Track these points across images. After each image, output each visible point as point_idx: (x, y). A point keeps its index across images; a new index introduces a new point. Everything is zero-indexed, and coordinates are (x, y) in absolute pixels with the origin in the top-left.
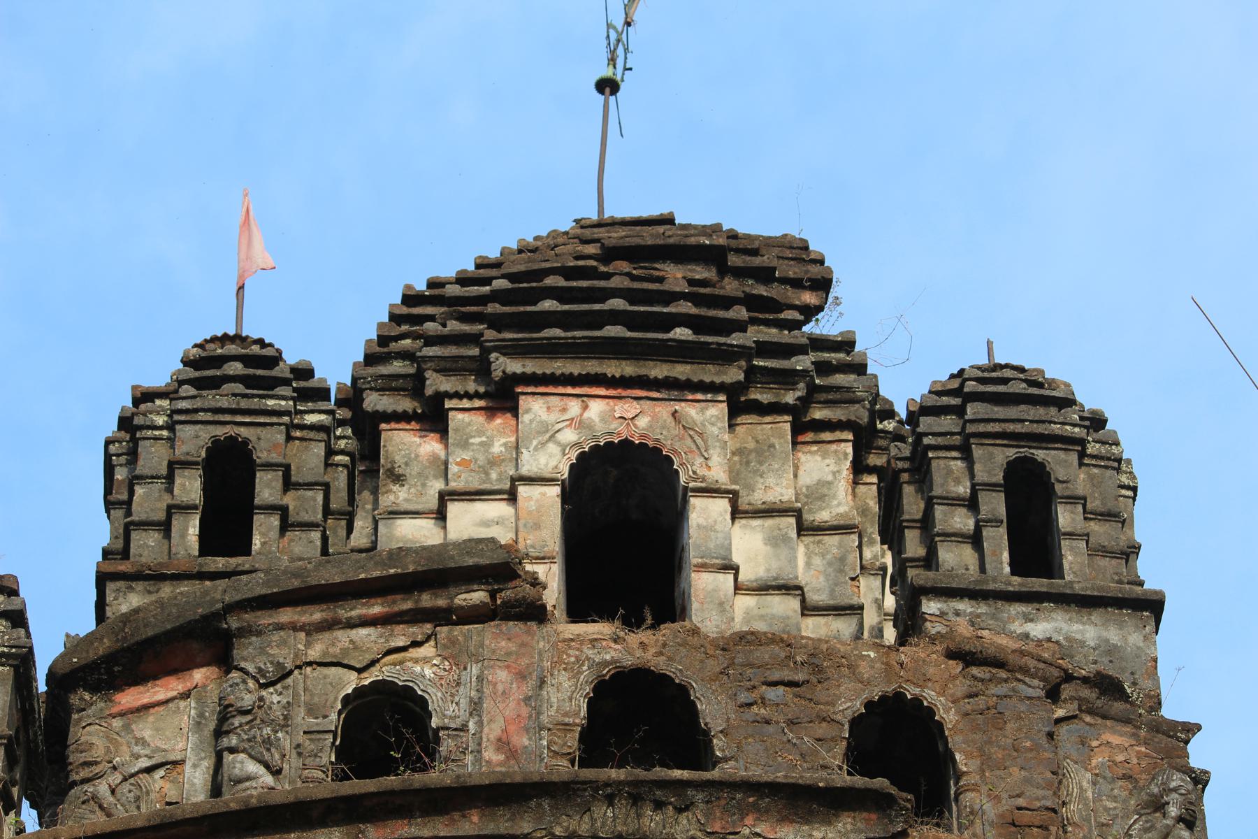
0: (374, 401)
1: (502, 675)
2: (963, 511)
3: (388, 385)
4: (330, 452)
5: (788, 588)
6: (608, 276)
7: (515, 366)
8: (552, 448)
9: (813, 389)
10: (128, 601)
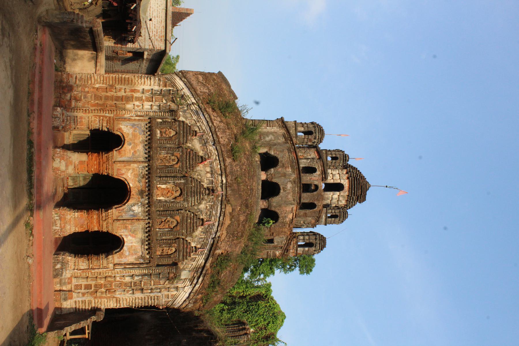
0: (348, 169)
1: (317, 178)
3: (350, 170)
5: (332, 199)
7: (350, 179)
9: (350, 202)
10: (324, 152)
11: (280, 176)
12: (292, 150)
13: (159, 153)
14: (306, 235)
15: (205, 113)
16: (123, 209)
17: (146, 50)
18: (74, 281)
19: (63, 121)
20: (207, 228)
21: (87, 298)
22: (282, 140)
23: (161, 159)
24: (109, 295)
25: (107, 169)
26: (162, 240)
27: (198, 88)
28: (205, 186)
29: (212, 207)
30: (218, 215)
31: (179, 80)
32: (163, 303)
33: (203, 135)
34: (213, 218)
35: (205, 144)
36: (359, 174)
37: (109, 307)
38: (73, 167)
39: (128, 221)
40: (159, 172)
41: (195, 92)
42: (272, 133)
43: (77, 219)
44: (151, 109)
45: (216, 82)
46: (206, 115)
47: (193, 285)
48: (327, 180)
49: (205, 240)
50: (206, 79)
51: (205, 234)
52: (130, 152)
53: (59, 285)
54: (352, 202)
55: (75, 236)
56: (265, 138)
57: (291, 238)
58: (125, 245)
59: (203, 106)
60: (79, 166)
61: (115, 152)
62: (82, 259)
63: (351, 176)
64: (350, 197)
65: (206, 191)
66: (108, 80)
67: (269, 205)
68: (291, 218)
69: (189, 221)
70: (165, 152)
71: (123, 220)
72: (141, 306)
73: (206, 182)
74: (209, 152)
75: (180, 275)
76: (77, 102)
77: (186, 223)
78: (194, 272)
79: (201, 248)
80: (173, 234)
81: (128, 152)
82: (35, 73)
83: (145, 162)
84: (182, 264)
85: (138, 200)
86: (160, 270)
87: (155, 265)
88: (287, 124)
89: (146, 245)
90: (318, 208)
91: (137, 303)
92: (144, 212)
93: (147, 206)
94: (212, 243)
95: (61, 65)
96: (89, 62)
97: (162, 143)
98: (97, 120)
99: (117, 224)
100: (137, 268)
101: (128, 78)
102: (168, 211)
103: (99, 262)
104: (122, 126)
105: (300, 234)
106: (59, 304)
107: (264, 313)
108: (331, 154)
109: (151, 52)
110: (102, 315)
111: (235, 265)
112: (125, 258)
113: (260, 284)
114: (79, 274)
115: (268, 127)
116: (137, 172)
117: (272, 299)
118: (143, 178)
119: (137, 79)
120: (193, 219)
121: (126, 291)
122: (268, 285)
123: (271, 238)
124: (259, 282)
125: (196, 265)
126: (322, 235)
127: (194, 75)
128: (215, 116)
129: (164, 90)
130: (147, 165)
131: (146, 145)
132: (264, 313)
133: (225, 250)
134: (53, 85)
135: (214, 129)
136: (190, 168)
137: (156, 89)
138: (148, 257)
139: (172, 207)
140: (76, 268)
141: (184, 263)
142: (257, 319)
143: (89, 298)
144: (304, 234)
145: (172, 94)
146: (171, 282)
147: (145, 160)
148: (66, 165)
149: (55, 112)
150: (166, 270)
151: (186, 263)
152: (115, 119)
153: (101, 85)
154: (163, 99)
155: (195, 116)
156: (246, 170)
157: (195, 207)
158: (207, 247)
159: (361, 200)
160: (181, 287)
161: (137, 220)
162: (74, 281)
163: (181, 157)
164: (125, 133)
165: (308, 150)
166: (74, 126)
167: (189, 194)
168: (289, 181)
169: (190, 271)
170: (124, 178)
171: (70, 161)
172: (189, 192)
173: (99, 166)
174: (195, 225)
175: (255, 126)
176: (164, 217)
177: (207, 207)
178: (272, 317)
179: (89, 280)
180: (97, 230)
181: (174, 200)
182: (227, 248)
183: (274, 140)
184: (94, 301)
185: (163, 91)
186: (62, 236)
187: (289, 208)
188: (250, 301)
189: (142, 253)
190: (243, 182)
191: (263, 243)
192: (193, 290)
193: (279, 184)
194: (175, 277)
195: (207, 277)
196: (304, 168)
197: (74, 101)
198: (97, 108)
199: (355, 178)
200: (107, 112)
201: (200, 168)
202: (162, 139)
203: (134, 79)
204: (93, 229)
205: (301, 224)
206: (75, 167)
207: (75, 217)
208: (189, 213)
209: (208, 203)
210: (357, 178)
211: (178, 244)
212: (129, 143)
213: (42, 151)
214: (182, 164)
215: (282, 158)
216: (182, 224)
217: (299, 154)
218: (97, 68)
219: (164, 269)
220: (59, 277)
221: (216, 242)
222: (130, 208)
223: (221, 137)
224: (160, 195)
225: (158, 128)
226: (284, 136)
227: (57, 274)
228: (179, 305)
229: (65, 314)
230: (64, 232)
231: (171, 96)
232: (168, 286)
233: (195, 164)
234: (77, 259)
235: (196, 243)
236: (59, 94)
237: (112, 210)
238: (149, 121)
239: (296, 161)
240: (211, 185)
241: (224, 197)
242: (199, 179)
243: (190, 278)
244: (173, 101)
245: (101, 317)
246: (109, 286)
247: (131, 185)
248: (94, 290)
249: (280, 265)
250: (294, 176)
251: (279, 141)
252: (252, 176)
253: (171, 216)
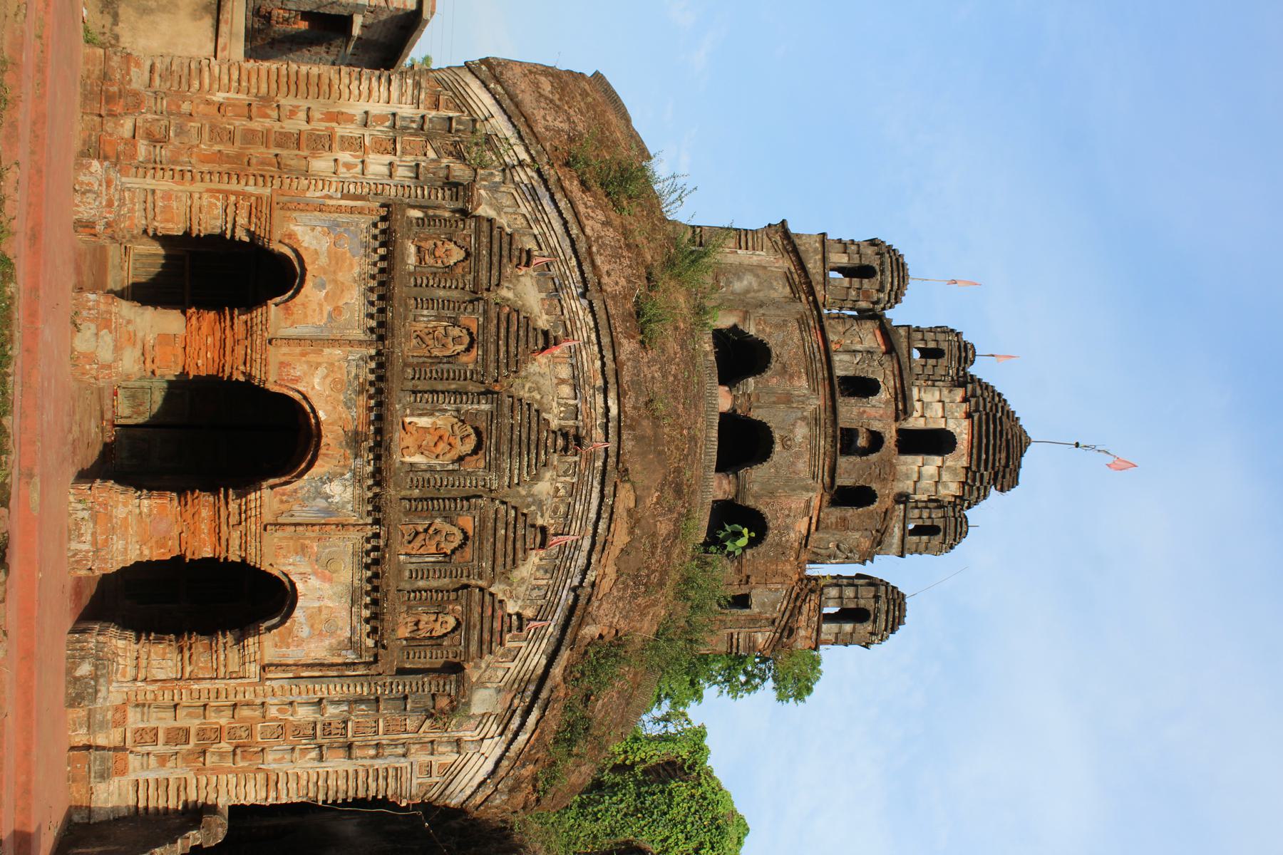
0: (970, 387)
1: (881, 412)
2: (928, 515)
3: (974, 390)
4: (944, 376)
5: (919, 478)
6: (1001, 440)
7: (976, 416)
8: (955, 426)
9: (972, 486)
10: (902, 332)
11: (774, 403)
12: (812, 323)
13: (411, 317)
14: (846, 586)
15: (558, 196)
16: (295, 491)
17: (359, 8)
18: (134, 719)
19: (110, 204)
20: (557, 558)
21: (174, 772)
22: (782, 291)
23: (418, 336)
24: (246, 764)
25: (245, 364)
26: (414, 591)
27: (539, 115)
28: (555, 424)
29: (573, 490)
30: (593, 515)
31: (480, 88)
32: (414, 792)
33: (552, 263)
34: (575, 526)
35: (557, 291)
36: (1000, 405)
37: (243, 802)
38: (138, 353)
39: (309, 528)
40: (411, 377)
41: (530, 126)
42: (752, 269)
43: (148, 520)
44: (391, 176)
45: (590, 100)
46: (560, 200)
47: (510, 736)
48: (911, 419)
49: (549, 593)
50: (563, 89)
51: (548, 575)
52: (321, 310)
53: (84, 730)
54: (978, 489)
55: (141, 568)
56: (731, 282)
57: (803, 595)
58: (298, 605)
59: (552, 172)
60: (156, 349)
61: (274, 309)
62: (161, 646)
63: (977, 410)
64: (975, 473)
65: (556, 441)
66: (254, 81)
67: (740, 489)
68: (804, 532)
69: (503, 532)
70: (433, 313)
71: (296, 525)
72: (345, 800)
73: (556, 411)
74: (567, 316)
75: (468, 704)
76: (155, 146)
77: (492, 540)
78: (512, 695)
79: (535, 620)
80: (451, 572)
81: (314, 310)
82: (22, 36)
83: (369, 344)
84: (477, 667)
85: (342, 463)
86: (407, 687)
87: (392, 670)
88: (797, 241)
89: (366, 606)
90: (880, 503)
91: (330, 787)
92: (362, 500)
93: (370, 482)
94: (570, 602)
95: (104, 26)
96: (195, 20)
97: (421, 286)
98: (219, 204)
99: (274, 538)
100: (336, 679)
101: (319, 76)
102: (438, 499)
103: (215, 657)
104: (296, 228)
105: (831, 581)
106: (83, 791)
107: (686, 816)
108: (923, 340)
109: (373, 15)
110: (221, 825)
111: (636, 674)
112: (298, 646)
113: (671, 729)
114: (150, 697)
115: (740, 248)
116: (342, 374)
117: (709, 774)
118: (360, 392)
119: (347, 81)
120: (515, 527)
121: (297, 751)
122: (695, 733)
123: (743, 590)
124: (669, 724)
125: (519, 672)
126: (894, 588)
127: (525, 75)
128: (589, 204)
129: (430, 119)
130: (373, 352)
131: (371, 290)
132: (686, 816)
133: (611, 627)
134: (79, 90)
135: (585, 245)
136: (507, 364)
137: (405, 115)
138: (370, 643)
139: (449, 487)
140: (141, 676)
141: (483, 666)
142: (667, 834)
143: (178, 770)
144: (840, 582)
145: (457, 131)
146: (440, 724)
147: (367, 338)
148: (116, 346)
149: (85, 175)
150: (428, 684)
151: (488, 666)
152: (274, 205)
153: (232, 95)
154: (429, 147)
155: (527, 204)
156: (679, 377)
157: (520, 489)
158: (556, 617)
159: (1005, 484)
161: (340, 527)
162: (134, 719)
163: (480, 332)
164: (306, 249)
165: (855, 324)
166: (144, 222)
167: (505, 448)
168: (800, 419)
169: (499, 690)
170: (299, 392)
171: (129, 333)
172: (505, 439)
173: (222, 351)
174: (519, 545)
175: (701, 244)
176: (425, 518)
177: (557, 490)
178: (709, 831)
179: (181, 713)
180: (211, 555)
181: (456, 466)
182: (616, 620)
183: (759, 291)
184: (195, 781)
185: (427, 121)
186: (98, 573)
187: (797, 503)
188: (645, 781)
189: (353, 629)
190: (669, 415)
191: (716, 607)
192: (507, 749)
193: (769, 427)
194: (453, 709)
195: (554, 709)
196: (845, 380)
197: (146, 142)
198: (217, 168)
199: (991, 417)
200: (252, 181)
201: (540, 366)
202: (422, 274)
203: (337, 82)
204: (196, 554)
205: (828, 552)
206: (143, 354)
207: (140, 513)
208: (503, 507)
209: (563, 479)
210: (994, 416)
211: (464, 602)
212: (318, 280)
213: (41, 293)
214: (485, 352)
215: (782, 347)
216: (481, 543)
217: (832, 337)
218: (221, 41)
219: (420, 683)
220: (86, 703)
221: (582, 601)
222: (316, 488)
223: (607, 272)
224: (412, 450)
225: (412, 236)
226: (788, 279)
227: (81, 693)
228: (465, 798)
229: (101, 823)
230: (105, 560)
231: (452, 139)
232: (431, 736)
233: (524, 355)
234: (143, 648)
235: (520, 603)
236: (97, 119)
237: (259, 493)
238: (383, 212)
239: (823, 358)
240: (571, 423)
241: (612, 460)
242: (536, 401)
243: (499, 711)
244: (460, 157)
245: (216, 834)
246: (244, 735)
247: (321, 414)
248: (197, 745)
249: (720, 674)
250: (816, 402)
251: (774, 295)
252: (696, 399)
253: (445, 517)
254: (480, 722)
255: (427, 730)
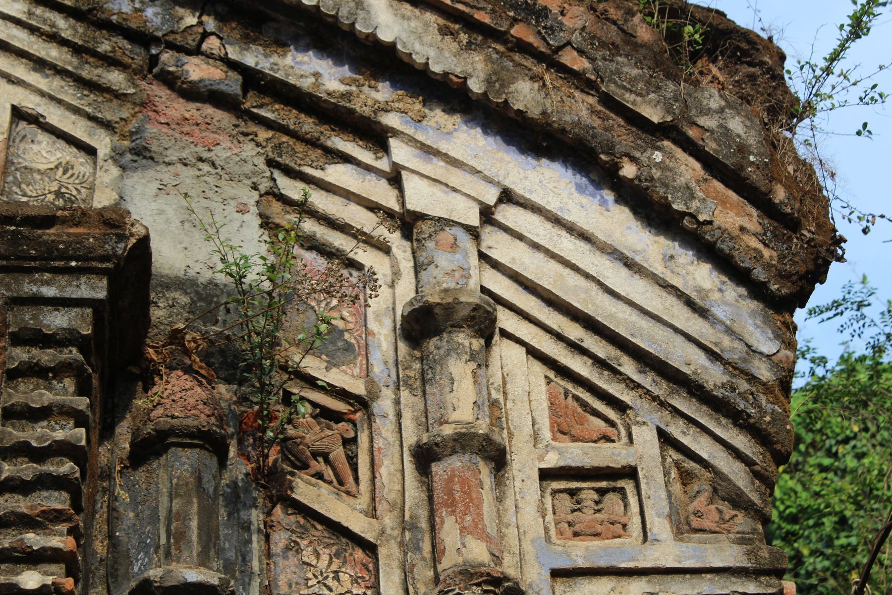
78: (160, 93)
107: (843, 472)
125: (40, 64)
160: (418, 268)
228: (733, 292)
254: (313, 244)
255: (363, 500)
